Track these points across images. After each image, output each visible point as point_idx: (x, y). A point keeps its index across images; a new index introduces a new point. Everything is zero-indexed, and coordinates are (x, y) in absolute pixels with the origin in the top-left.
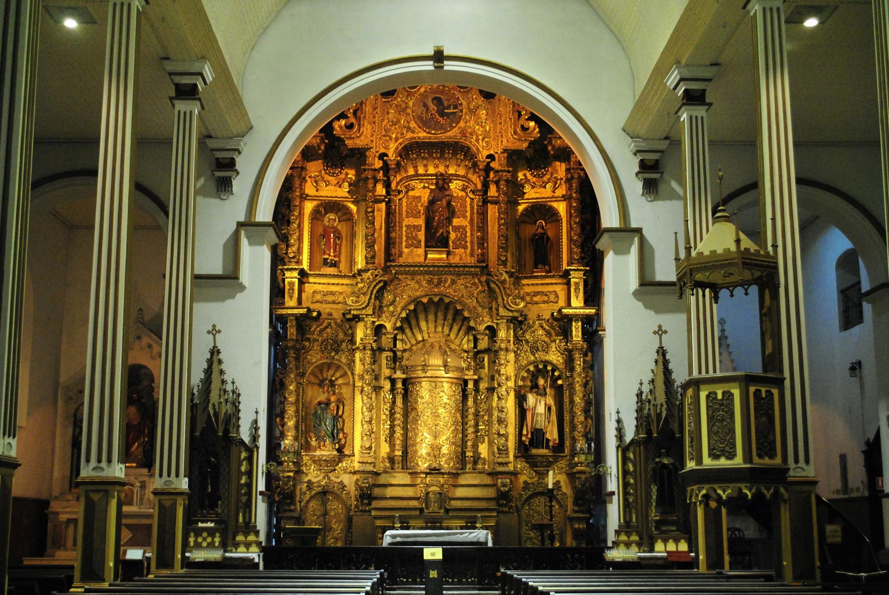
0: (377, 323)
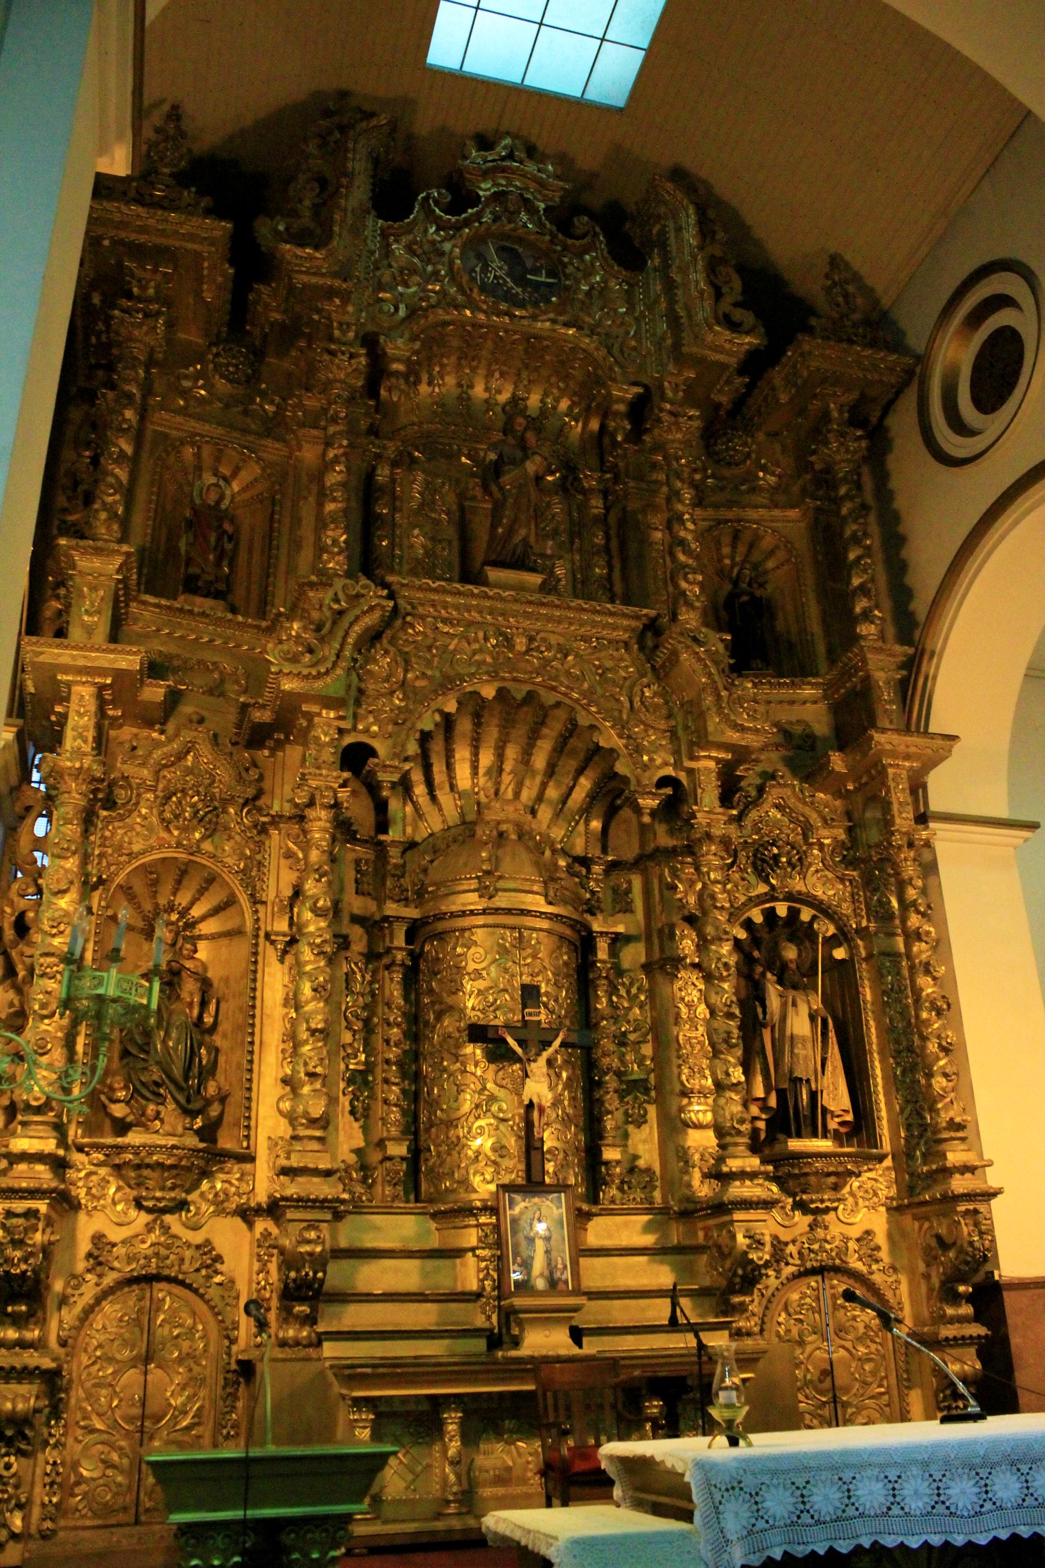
0: (348, 740)
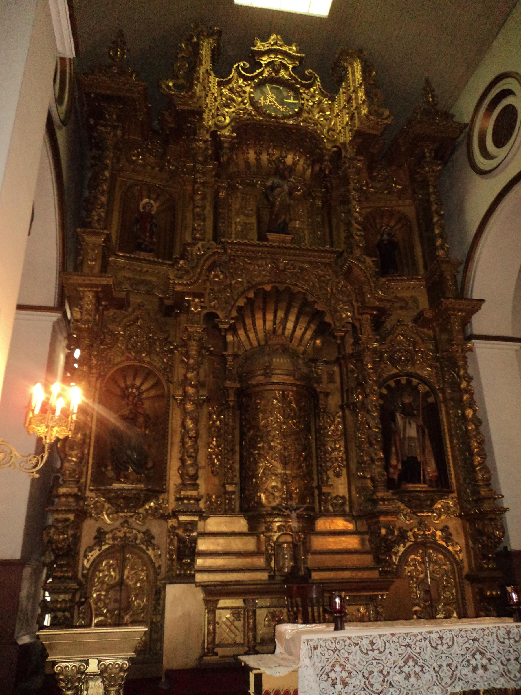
0: (205, 311)
